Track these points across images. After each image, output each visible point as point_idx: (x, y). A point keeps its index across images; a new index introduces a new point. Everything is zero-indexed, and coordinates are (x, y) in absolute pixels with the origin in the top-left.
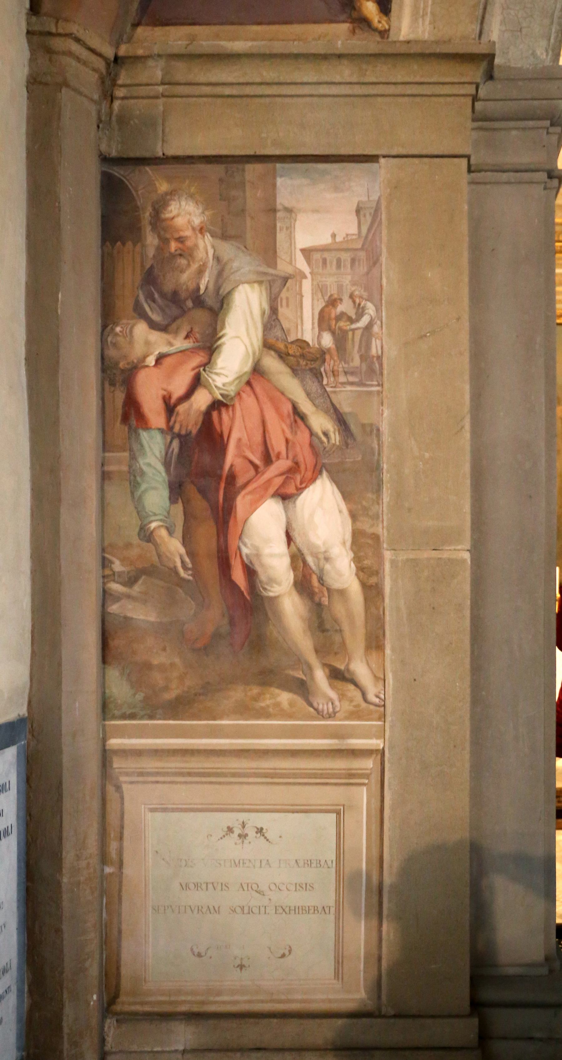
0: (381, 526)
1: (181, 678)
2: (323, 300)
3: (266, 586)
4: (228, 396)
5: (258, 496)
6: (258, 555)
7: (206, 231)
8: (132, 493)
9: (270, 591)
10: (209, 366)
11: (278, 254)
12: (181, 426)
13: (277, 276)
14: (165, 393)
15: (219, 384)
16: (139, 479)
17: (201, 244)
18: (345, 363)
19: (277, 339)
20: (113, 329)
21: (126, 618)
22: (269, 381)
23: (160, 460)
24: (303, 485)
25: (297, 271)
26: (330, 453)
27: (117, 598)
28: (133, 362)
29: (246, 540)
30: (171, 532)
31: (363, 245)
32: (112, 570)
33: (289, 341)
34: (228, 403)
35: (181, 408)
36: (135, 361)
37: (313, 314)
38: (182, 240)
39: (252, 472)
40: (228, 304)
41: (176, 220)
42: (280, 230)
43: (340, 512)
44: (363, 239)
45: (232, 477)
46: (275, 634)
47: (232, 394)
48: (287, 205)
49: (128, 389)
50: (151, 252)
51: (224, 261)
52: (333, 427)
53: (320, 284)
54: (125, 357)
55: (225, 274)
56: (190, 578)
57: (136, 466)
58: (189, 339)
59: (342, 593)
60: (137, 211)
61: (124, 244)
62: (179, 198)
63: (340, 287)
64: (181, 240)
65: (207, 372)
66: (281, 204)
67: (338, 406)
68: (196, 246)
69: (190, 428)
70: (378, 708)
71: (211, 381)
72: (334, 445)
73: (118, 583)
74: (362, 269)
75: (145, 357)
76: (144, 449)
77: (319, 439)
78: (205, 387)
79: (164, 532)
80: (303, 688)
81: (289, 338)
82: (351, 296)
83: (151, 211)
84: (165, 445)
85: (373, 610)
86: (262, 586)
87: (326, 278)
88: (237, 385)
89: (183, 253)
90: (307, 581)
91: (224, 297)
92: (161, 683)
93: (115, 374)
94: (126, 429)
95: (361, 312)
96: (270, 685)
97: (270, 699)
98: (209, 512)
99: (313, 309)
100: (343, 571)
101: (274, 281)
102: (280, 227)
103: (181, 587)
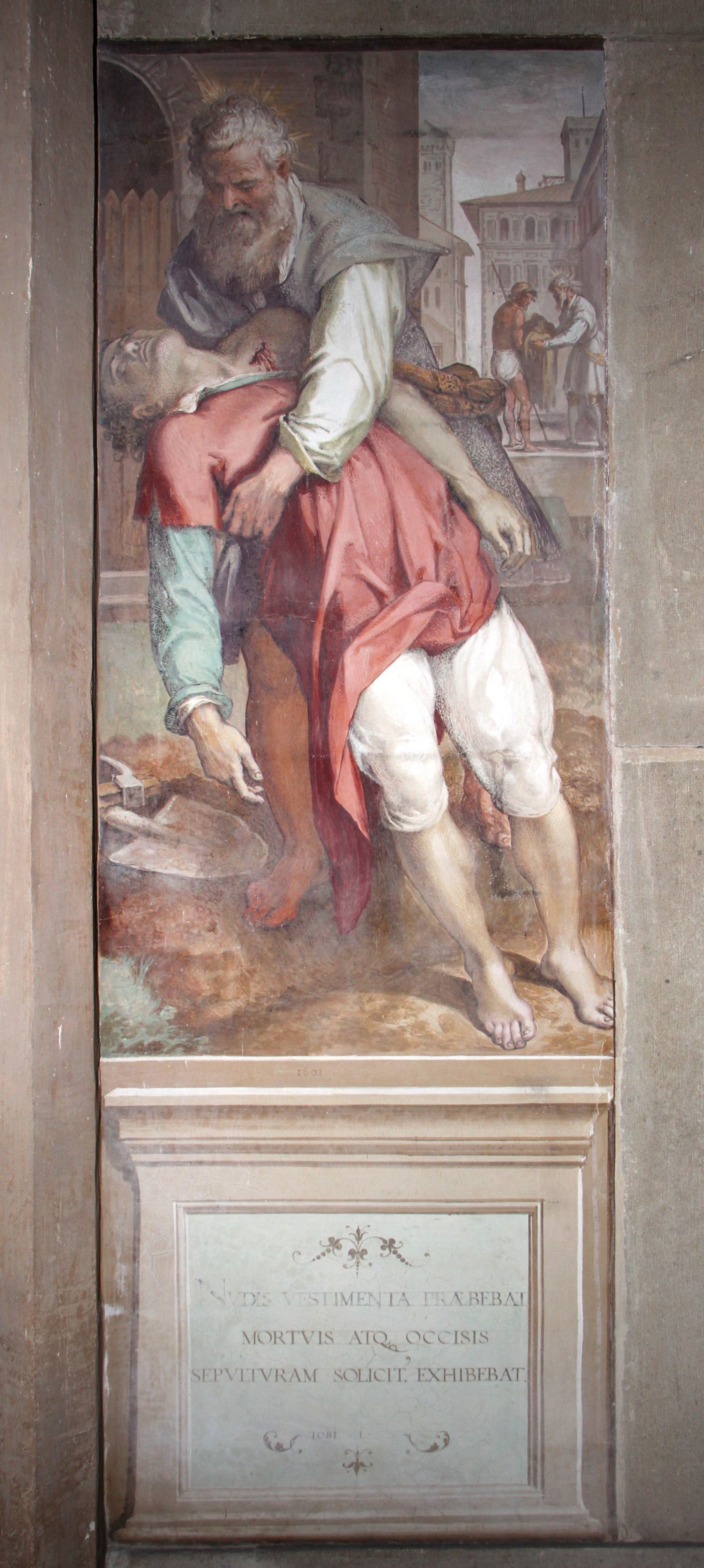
0: (606, 703)
1: (244, 980)
2: (502, 294)
3: (397, 814)
4: (329, 466)
5: (383, 648)
6: (383, 757)
7: (291, 171)
8: (155, 645)
9: (404, 821)
10: (294, 412)
11: (421, 212)
12: (243, 521)
13: (419, 251)
14: (215, 462)
15: (314, 446)
16: (166, 618)
17: (281, 192)
18: (541, 408)
19: (419, 364)
20: (120, 347)
21: (143, 872)
22: (403, 439)
23: (205, 584)
24: (467, 629)
25: (456, 241)
26: (513, 570)
27: (126, 836)
28: (157, 404)
29: (362, 729)
30: (224, 718)
31: (573, 197)
32: (117, 785)
34: (330, 480)
35: (243, 490)
36: (161, 404)
37: (484, 318)
38: (246, 186)
39: (373, 605)
40: (330, 301)
41: (235, 150)
42: (425, 169)
43: (533, 677)
44: (573, 186)
45: (336, 615)
46: (416, 899)
47: (337, 462)
48: (437, 125)
49: (147, 456)
50: (190, 209)
51: (324, 224)
52: (520, 521)
53: (497, 264)
54: (143, 397)
55: (325, 247)
56: (260, 799)
57: (163, 595)
58: (259, 363)
59: (537, 824)
60: (164, 136)
61: (141, 194)
62: (242, 111)
63: (533, 272)
64: (245, 187)
65: (292, 424)
66: (426, 122)
67: (528, 485)
68: (273, 197)
69: (259, 525)
70: (602, 1032)
71: (298, 439)
72: (521, 555)
73: (128, 809)
75: (178, 397)
76: (176, 564)
77: (495, 544)
78: (288, 450)
79: (211, 716)
80: (466, 996)
81: (440, 363)
82: (552, 288)
83: (190, 133)
84: (215, 558)
85: (592, 856)
86: (390, 814)
87: (507, 254)
88: (346, 446)
89: (249, 210)
90: (473, 806)
91: (323, 287)
92: (207, 989)
93: (123, 428)
94: (144, 527)
95: (569, 317)
96: (407, 992)
97: (405, 1018)
98: (295, 678)
99: (484, 310)
100: (536, 786)
101: (413, 259)
102: (425, 163)
103: (242, 816)
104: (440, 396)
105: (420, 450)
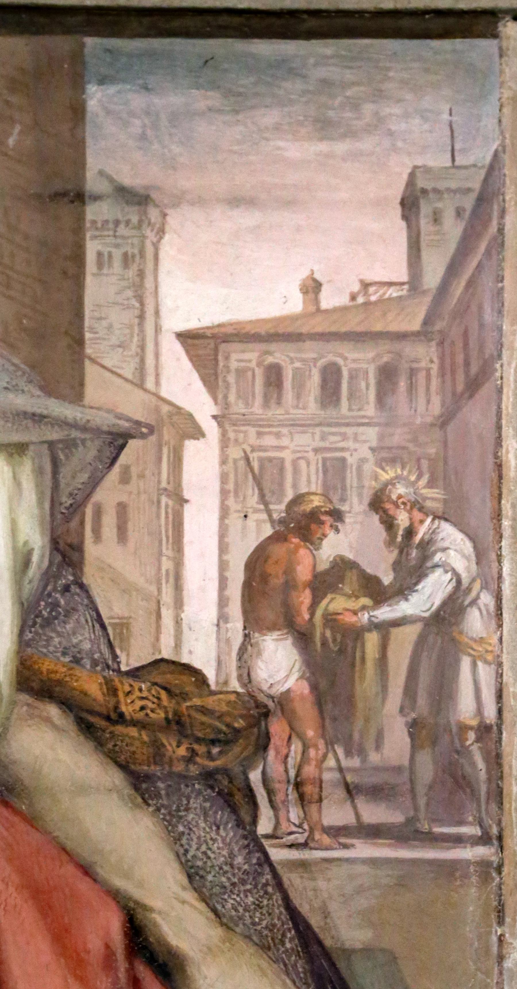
13: (84, 429)
19: (77, 661)
22: (32, 821)
33: (124, 668)
42: (100, 265)
48: (127, 181)
66: (101, 173)
74: (429, 405)
81: (123, 658)
102: (100, 254)
104: (119, 729)
105: (69, 845)
